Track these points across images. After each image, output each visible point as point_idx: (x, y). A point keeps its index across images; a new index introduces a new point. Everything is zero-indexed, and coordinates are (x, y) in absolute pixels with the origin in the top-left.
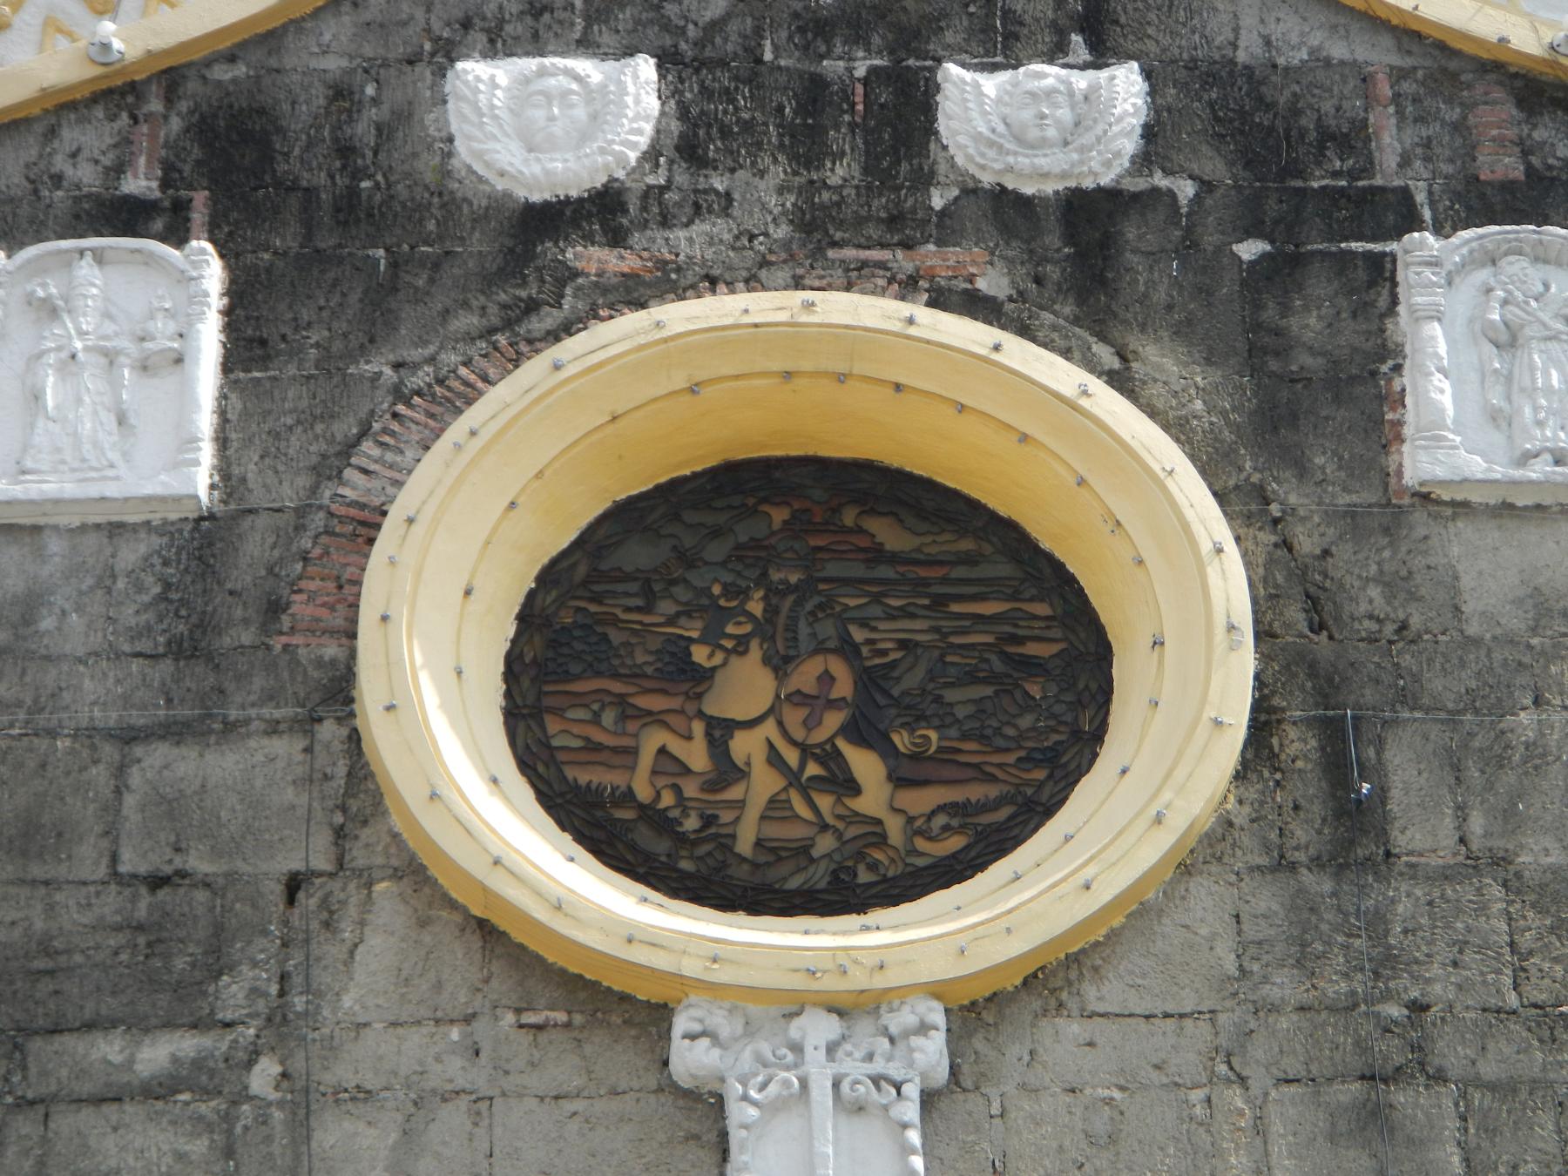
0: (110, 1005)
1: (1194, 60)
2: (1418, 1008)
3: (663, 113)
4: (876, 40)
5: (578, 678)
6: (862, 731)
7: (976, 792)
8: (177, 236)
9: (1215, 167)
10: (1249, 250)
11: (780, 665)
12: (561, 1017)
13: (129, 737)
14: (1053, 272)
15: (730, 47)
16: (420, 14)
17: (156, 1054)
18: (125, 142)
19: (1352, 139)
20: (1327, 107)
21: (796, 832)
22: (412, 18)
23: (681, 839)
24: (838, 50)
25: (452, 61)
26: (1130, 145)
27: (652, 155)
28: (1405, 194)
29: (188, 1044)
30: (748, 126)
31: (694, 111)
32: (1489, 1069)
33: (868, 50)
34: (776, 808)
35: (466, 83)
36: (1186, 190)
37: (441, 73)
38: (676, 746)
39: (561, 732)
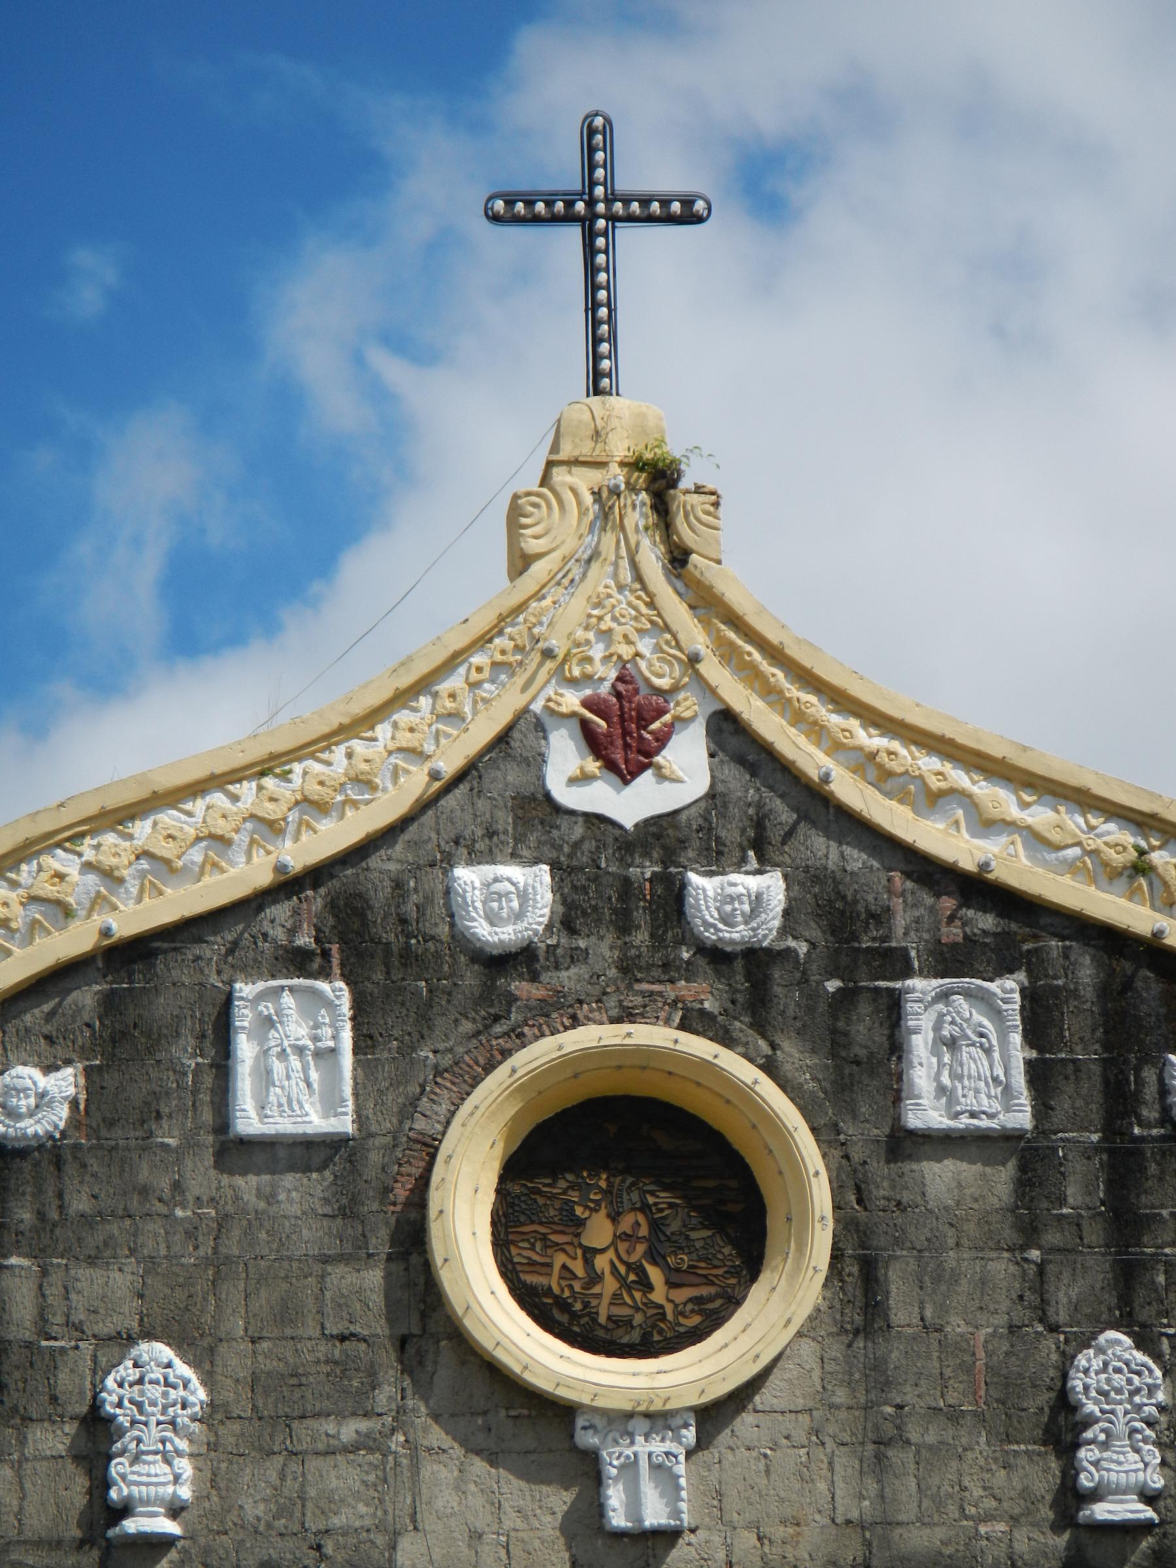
0: (327, 1405)
1: (807, 866)
2: (900, 1407)
3: (554, 901)
4: (655, 855)
5: (524, 1224)
6: (654, 1256)
7: (705, 1291)
8: (324, 973)
9: (815, 933)
10: (832, 985)
11: (614, 1217)
12: (525, 1412)
13: (325, 1260)
14: (740, 998)
15: (585, 859)
16: (434, 836)
17: (350, 1430)
18: (296, 912)
19: (881, 917)
20: (870, 898)
21: (626, 1311)
22: (430, 838)
23: (574, 1316)
24: (638, 861)
25: (452, 866)
26: (777, 923)
27: (549, 927)
28: (905, 952)
29: (364, 1425)
30: (595, 908)
31: (569, 900)
32: (931, 1438)
33: (651, 861)
34: (616, 1298)
35: (459, 885)
36: (802, 948)
37: (446, 872)
38: (570, 1264)
39: (519, 1254)
